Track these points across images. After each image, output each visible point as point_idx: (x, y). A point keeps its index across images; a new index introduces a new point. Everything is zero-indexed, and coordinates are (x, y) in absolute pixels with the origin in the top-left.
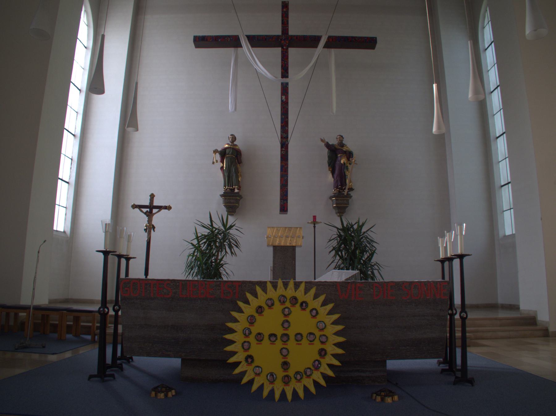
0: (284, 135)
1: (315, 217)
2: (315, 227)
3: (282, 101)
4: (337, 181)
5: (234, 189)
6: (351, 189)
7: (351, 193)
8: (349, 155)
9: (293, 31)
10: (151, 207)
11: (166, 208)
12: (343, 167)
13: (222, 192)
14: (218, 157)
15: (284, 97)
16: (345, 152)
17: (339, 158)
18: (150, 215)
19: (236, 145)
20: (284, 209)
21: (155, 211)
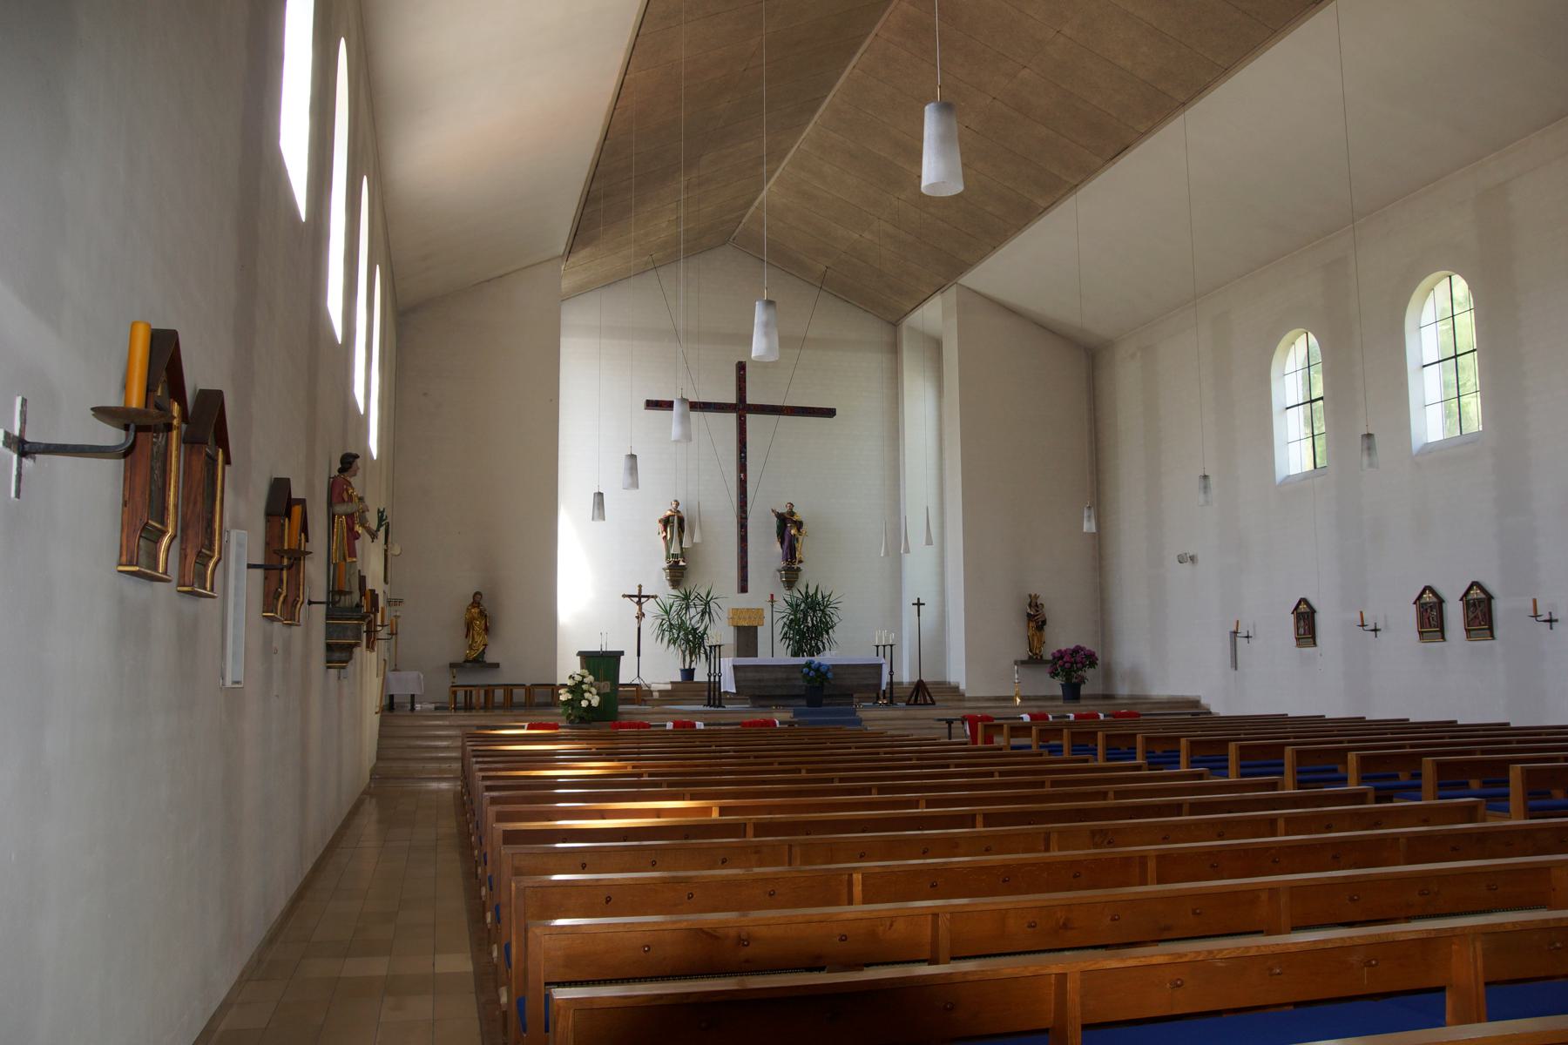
0: (744, 516)
1: (772, 596)
2: (772, 606)
3: (741, 479)
4: (787, 554)
5: (679, 562)
6: (800, 562)
7: (800, 566)
8: (799, 525)
9: (750, 400)
10: (640, 596)
11: (653, 597)
12: (793, 539)
13: (665, 565)
14: (660, 527)
15: (742, 475)
16: (795, 522)
17: (789, 529)
18: (639, 603)
19: (678, 512)
20: (743, 588)
21: (643, 600)
